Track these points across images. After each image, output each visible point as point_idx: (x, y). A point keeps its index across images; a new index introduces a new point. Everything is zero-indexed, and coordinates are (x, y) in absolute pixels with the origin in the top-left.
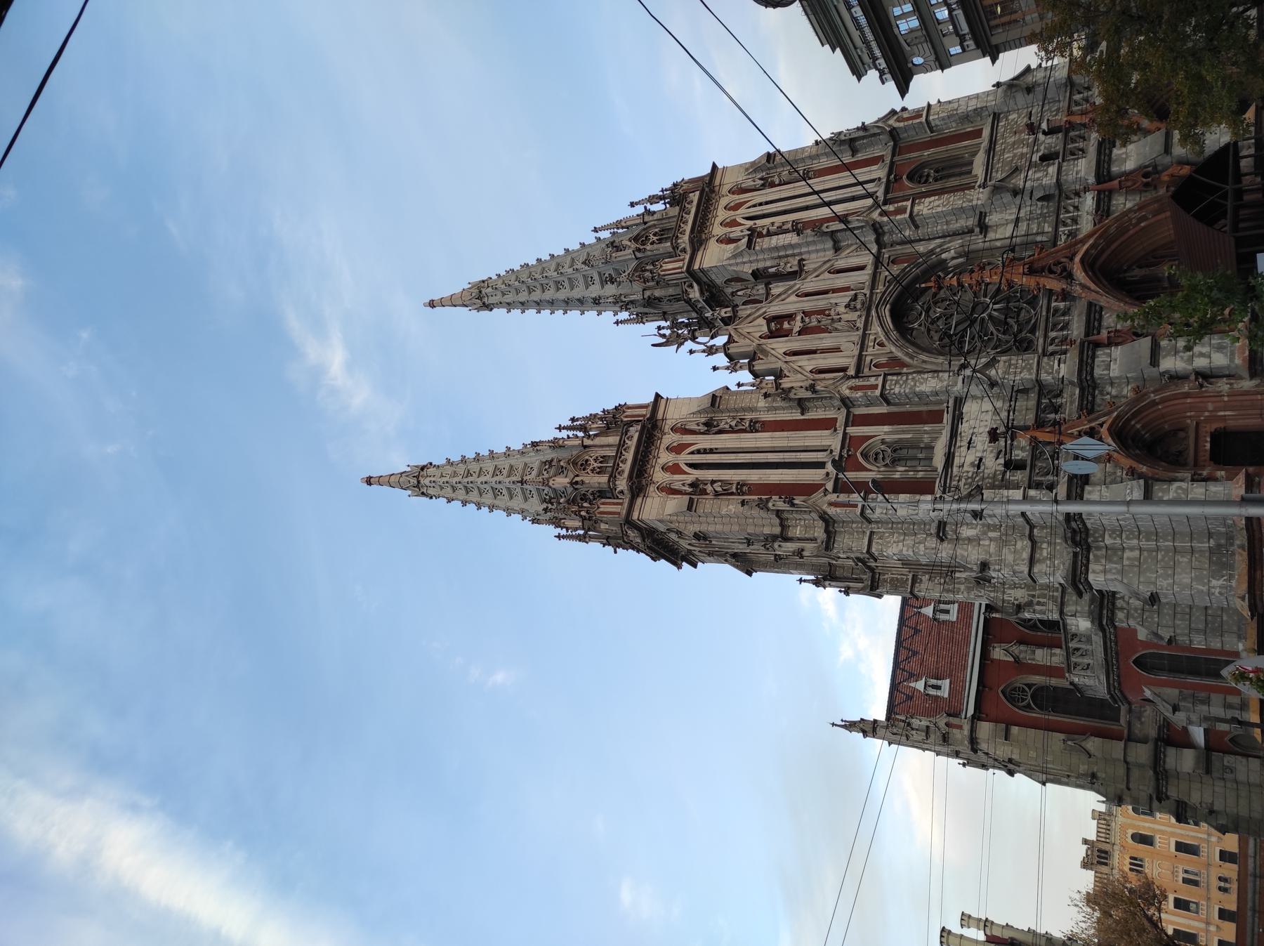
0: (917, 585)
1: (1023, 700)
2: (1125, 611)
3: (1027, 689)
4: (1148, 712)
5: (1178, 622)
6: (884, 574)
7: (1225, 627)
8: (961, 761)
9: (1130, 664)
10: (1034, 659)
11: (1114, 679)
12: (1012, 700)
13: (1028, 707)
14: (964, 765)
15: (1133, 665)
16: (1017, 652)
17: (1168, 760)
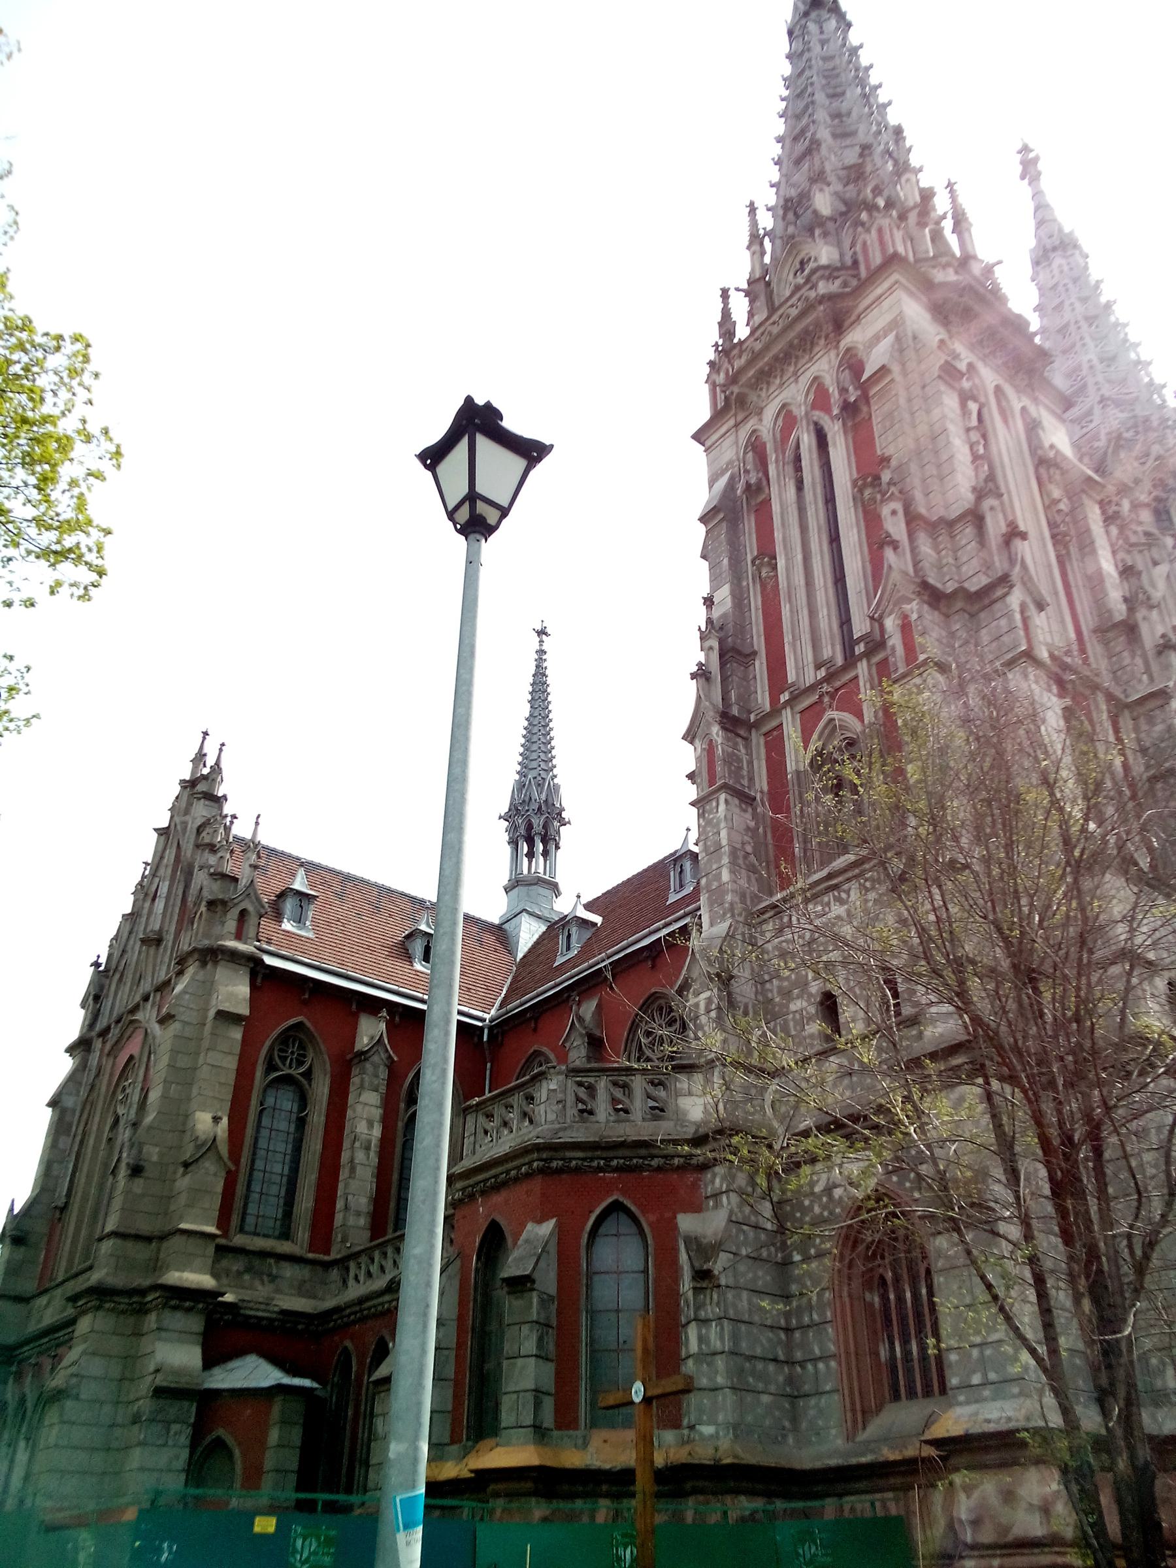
0: (737, 801)
1: (284, 1059)
2: (750, 1189)
3: (301, 1070)
4: (260, 1288)
5: (745, 1294)
6: (748, 746)
7: (749, 1398)
8: (103, 960)
9: (609, 1193)
10: (362, 1087)
11: (571, 1159)
12: (285, 1039)
13: (271, 1067)
14: (96, 964)
15: (610, 1200)
16: (375, 1058)
17: (179, 1315)
